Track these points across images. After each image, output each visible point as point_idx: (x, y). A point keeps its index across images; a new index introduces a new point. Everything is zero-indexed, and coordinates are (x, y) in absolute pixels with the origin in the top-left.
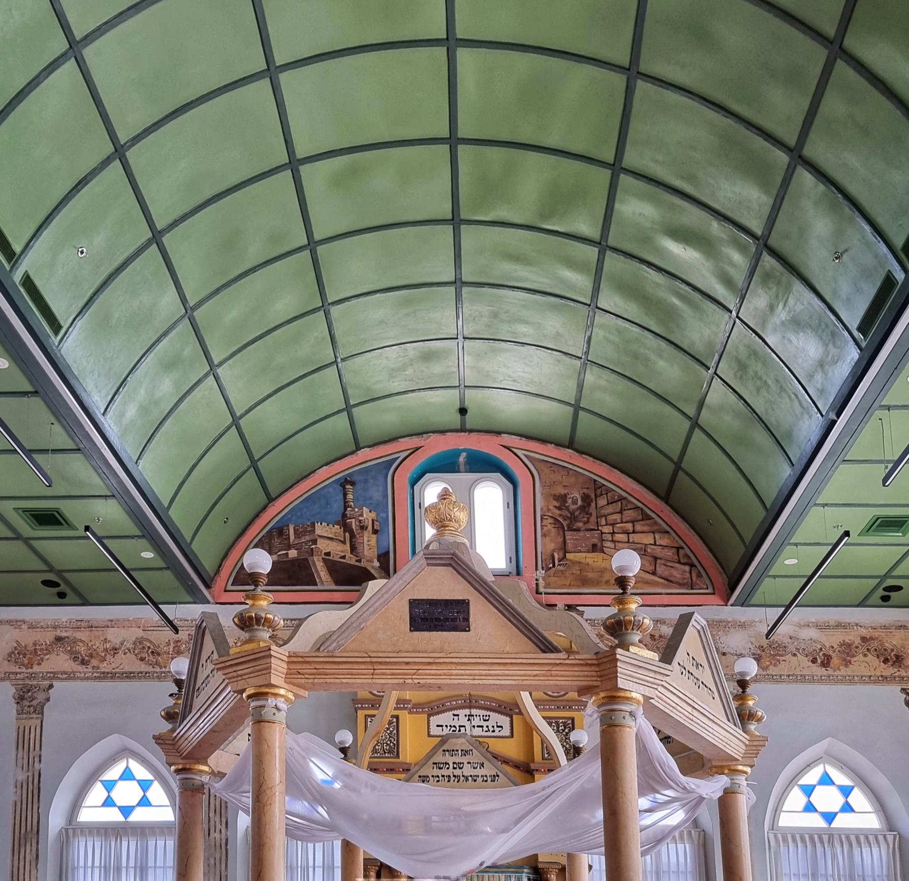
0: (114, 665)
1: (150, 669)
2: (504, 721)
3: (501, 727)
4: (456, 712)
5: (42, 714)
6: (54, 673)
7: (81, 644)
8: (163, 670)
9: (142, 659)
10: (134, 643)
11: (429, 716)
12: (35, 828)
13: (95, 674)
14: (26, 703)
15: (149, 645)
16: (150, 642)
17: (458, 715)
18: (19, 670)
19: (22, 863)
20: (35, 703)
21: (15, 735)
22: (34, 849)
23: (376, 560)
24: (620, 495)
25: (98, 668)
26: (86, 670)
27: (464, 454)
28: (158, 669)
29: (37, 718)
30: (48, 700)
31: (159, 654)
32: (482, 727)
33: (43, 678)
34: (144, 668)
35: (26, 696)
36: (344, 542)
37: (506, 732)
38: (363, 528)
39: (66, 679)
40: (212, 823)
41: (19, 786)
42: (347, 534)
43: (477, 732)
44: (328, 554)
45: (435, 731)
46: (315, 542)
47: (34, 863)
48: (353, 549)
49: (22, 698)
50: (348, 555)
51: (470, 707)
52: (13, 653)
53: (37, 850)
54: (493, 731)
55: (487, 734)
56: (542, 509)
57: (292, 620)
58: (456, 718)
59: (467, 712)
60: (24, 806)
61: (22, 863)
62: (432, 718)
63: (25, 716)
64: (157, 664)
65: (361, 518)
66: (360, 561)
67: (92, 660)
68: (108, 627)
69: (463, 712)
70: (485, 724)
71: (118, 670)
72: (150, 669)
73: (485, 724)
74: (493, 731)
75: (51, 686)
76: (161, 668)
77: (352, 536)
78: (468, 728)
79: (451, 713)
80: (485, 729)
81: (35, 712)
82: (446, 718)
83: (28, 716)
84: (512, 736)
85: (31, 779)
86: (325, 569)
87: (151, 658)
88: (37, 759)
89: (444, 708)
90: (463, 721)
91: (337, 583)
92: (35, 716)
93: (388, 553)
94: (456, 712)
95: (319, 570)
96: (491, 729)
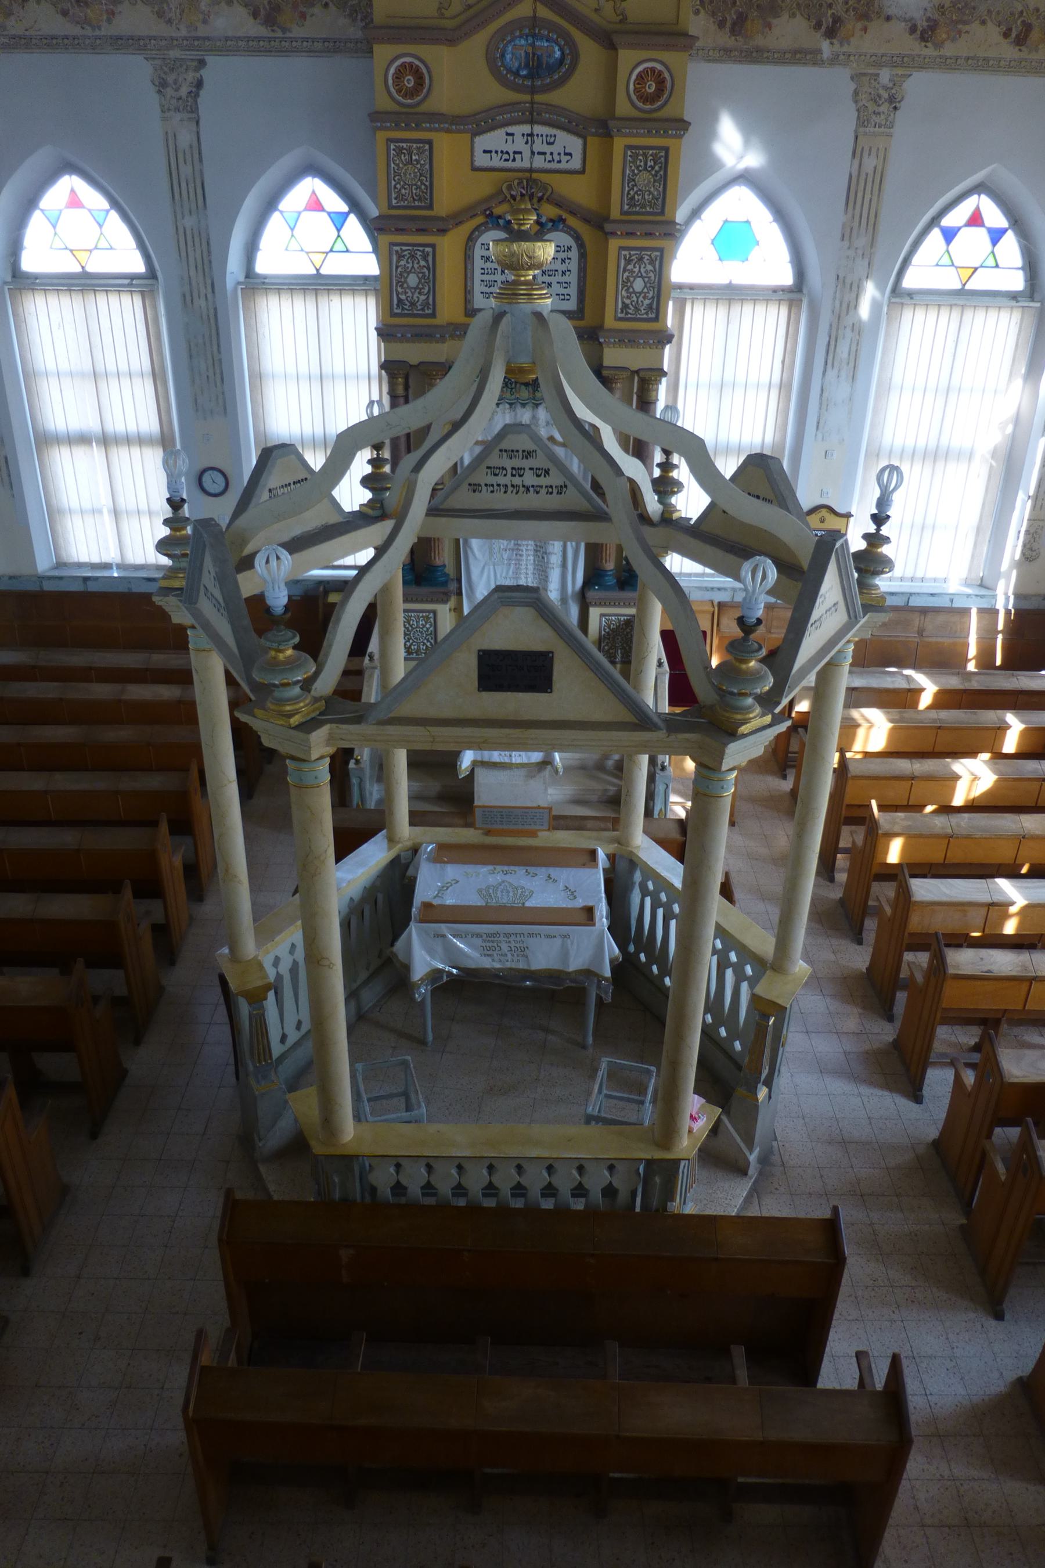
1: (76, 31)
2: (574, 143)
3: (570, 154)
8: (97, 33)
9: (65, 13)
11: (475, 134)
17: (512, 135)
28: (89, 31)
32: (544, 154)
37: (576, 163)
40: (194, 283)
43: (539, 162)
45: (482, 160)
51: (532, 122)
54: (559, 162)
55: (554, 166)
58: (510, 138)
59: (526, 129)
62: (478, 139)
64: (86, 22)
70: (547, 149)
72: (76, 31)
73: (547, 149)
74: (559, 162)
76: (94, 29)
78: (527, 154)
80: (548, 157)
90: (520, 144)
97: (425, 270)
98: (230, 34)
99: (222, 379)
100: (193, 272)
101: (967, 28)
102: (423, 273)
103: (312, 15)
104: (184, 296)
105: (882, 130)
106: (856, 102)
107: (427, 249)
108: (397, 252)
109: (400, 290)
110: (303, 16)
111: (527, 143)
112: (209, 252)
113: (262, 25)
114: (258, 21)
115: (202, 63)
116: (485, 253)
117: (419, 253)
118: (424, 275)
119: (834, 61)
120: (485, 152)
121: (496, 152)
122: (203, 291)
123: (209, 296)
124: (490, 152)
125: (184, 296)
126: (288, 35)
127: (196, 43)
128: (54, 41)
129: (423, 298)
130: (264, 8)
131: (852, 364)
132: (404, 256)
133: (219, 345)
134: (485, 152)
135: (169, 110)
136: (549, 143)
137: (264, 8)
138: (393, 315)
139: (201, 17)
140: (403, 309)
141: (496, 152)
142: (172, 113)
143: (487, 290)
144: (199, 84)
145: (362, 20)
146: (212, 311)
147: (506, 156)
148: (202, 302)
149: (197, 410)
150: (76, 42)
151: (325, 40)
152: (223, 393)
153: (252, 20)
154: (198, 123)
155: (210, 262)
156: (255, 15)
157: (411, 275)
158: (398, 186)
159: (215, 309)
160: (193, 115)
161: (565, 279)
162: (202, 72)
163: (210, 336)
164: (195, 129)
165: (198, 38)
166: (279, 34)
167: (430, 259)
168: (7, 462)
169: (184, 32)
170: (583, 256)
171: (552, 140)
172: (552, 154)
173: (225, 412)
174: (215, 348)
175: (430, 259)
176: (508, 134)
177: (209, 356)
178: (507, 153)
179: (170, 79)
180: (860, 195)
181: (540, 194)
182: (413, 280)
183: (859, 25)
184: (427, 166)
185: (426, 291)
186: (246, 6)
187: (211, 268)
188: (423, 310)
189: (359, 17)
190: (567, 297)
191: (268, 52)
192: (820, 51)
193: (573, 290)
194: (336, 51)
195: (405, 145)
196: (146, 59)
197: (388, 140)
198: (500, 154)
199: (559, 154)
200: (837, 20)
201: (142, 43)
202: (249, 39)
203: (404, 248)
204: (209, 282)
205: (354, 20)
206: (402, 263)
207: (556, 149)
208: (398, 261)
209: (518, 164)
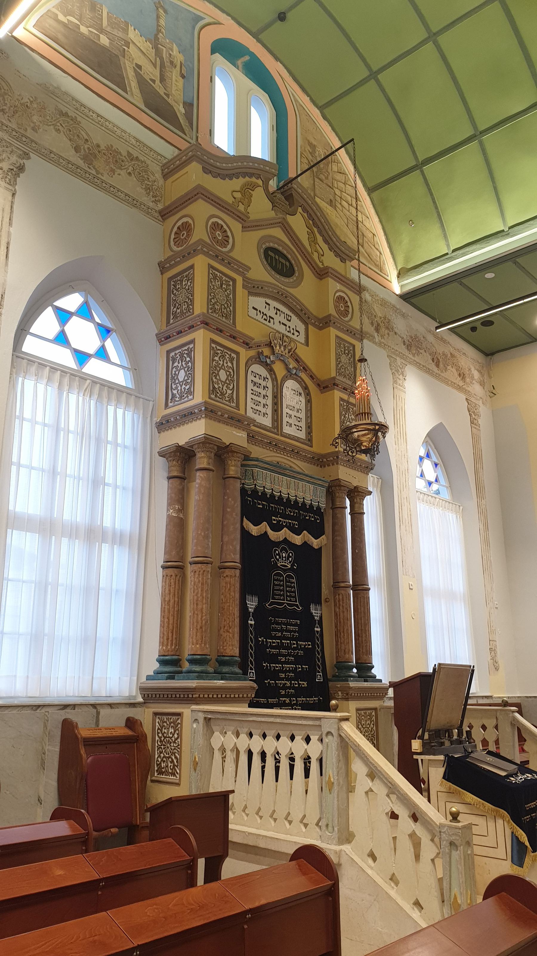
4: (269, 301)
17: (269, 305)
23: (181, 106)
24: (344, 170)
27: (247, 58)
32: (286, 325)
36: (155, 65)
37: (302, 338)
38: (172, 63)
42: (158, 59)
43: (282, 329)
44: (140, 67)
46: (127, 44)
48: (162, 79)
50: (158, 82)
54: (293, 334)
56: (301, 147)
57: (98, 115)
58: (267, 306)
65: (171, 52)
66: (168, 95)
69: (274, 304)
77: (162, 66)
79: (264, 299)
80: (288, 329)
82: (258, 302)
84: (307, 344)
86: (135, 81)
89: (262, 291)
91: (147, 105)
93: (191, 105)
94: (269, 301)
95: (130, 78)
96: (292, 331)
97: (231, 371)
98: (54, 150)
101: (421, 351)
102: (230, 372)
103: (119, 174)
105: (402, 388)
106: (391, 369)
107: (233, 355)
108: (213, 348)
109: (214, 380)
110: (113, 171)
111: (276, 314)
113: (81, 159)
114: (78, 155)
115: (26, 156)
116: (254, 379)
117: (228, 356)
118: (230, 374)
119: (380, 344)
120: (253, 308)
121: (260, 311)
124: (257, 310)
126: (100, 176)
127: (24, 139)
129: (229, 392)
130: (84, 150)
131: (410, 523)
132: (217, 353)
134: (253, 308)
136: (288, 320)
137: (84, 150)
138: (210, 398)
139: (32, 125)
140: (216, 396)
141: (260, 311)
143: (254, 407)
144: (21, 169)
145: (153, 197)
147: (265, 317)
151: (126, 195)
153: (73, 151)
154: (14, 195)
156: (77, 149)
157: (222, 370)
158: (212, 300)
160: (11, 187)
161: (298, 415)
162: (24, 161)
164: (10, 198)
165: (27, 137)
166: (94, 172)
167: (235, 363)
169: (14, 126)
170: (309, 401)
171: (289, 318)
172: (289, 327)
175: (235, 363)
176: (266, 303)
178: (266, 315)
180: (398, 420)
181: (290, 348)
182: (223, 375)
183: (387, 331)
184: (231, 296)
185: (231, 387)
186: (70, 140)
188: (229, 401)
189: (151, 193)
190: (300, 429)
191: (84, 179)
192: (374, 337)
193: (303, 424)
194: (135, 206)
195: (218, 274)
197: (209, 264)
198: (262, 315)
199: (293, 329)
200: (378, 325)
202: (69, 162)
203: (218, 348)
205: (148, 194)
206: (217, 358)
207: (292, 324)
208: (214, 356)
209: (271, 325)
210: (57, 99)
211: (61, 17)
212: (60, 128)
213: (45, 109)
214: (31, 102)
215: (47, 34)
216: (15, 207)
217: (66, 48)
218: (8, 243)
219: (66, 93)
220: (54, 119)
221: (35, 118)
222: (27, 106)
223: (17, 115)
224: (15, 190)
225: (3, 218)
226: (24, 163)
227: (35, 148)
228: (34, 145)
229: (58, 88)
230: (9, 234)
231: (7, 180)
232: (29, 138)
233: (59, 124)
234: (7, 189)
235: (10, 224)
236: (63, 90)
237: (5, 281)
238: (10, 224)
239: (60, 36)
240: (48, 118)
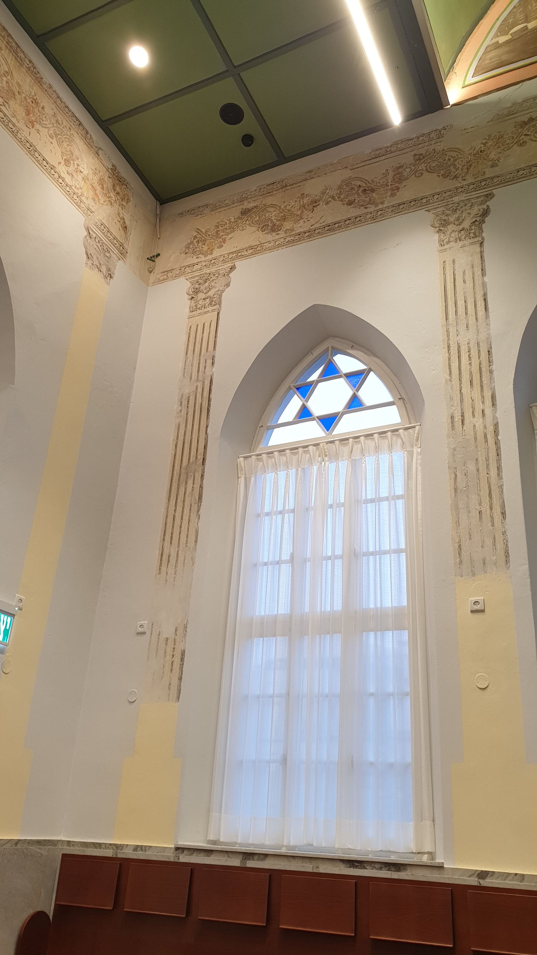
0: (312, 221)
5: (220, 304)
6: (237, 252)
7: (272, 209)
8: (381, 206)
9: (350, 203)
10: (340, 187)
12: (200, 457)
13: (288, 239)
14: (201, 296)
15: (359, 183)
16: (361, 179)
18: (196, 261)
19: (179, 509)
20: (211, 293)
21: (185, 338)
22: (197, 486)
25: (292, 230)
26: (277, 237)
29: (213, 311)
30: (228, 285)
31: (373, 190)
33: (224, 261)
34: (353, 212)
35: (202, 288)
39: (252, 254)
41: (185, 403)
47: (195, 508)
49: (197, 291)
52: (192, 243)
53: (201, 487)
60: (189, 427)
61: (179, 509)
63: (199, 311)
64: (372, 202)
67: (285, 223)
68: (306, 180)
71: (317, 225)
75: (233, 268)
76: (377, 205)
81: (210, 304)
83: (204, 310)
85: (200, 390)
87: (363, 197)
88: (209, 362)
92: (210, 309)
99: (503, 514)
100: (466, 389)
104: (452, 417)
112: (490, 362)
115: (490, 196)
122: (479, 407)
123: (488, 412)
125: (452, 417)
128: (337, 226)
133: (499, 468)
135: (449, 242)
139: (491, 163)
142: (452, 244)
144: (486, 213)
146: (491, 428)
148: (478, 422)
149: (461, 562)
150: (357, 220)
152: (504, 533)
154: (481, 244)
155: (491, 372)
159: (496, 425)
160: (476, 239)
163: (487, 460)
164: (478, 249)
168: (182, 660)
169: (470, 179)
173: (507, 562)
174: (493, 472)
177: (484, 484)
179: (452, 219)
187: (491, 379)
196: (428, 211)
201: (424, 200)
204: (488, 395)
210: (515, 115)
211: (502, 39)
212: (526, 138)
213: (502, 137)
214: (484, 144)
215: (489, 69)
216: (485, 255)
217: (514, 60)
218: (485, 295)
219: (525, 101)
220: (515, 137)
221: (492, 155)
222: (481, 151)
223: (472, 168)
224: (483, 239)
225: (473, 274)
226: (488, 206)
227: (498, 183)
228: (495, 181)
229: (514, 104)
230: (484, 285)
231: (472, 235)
232: (488, 178)
233: (523, 137)
234: (472, 244)
235: (483, 274)
236: (520, 100)
237: (489, 335)
238: (483, 274)
239: (504, 57)
240: (508, 142)
